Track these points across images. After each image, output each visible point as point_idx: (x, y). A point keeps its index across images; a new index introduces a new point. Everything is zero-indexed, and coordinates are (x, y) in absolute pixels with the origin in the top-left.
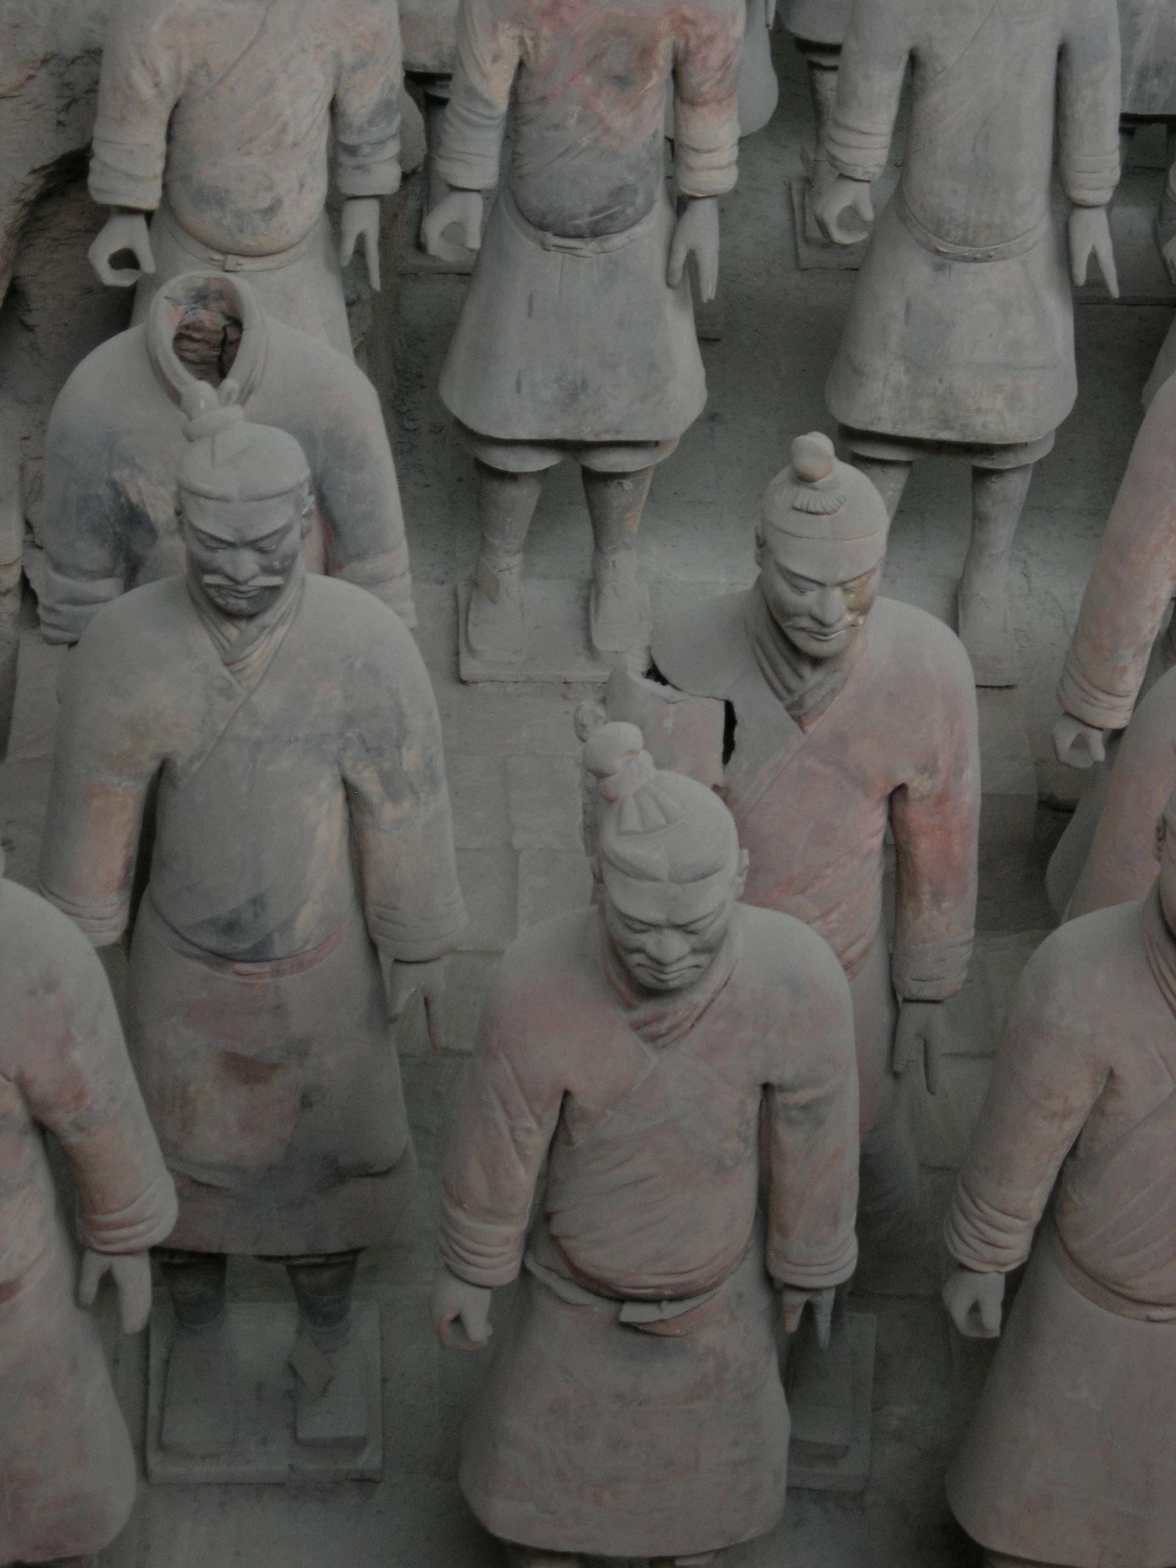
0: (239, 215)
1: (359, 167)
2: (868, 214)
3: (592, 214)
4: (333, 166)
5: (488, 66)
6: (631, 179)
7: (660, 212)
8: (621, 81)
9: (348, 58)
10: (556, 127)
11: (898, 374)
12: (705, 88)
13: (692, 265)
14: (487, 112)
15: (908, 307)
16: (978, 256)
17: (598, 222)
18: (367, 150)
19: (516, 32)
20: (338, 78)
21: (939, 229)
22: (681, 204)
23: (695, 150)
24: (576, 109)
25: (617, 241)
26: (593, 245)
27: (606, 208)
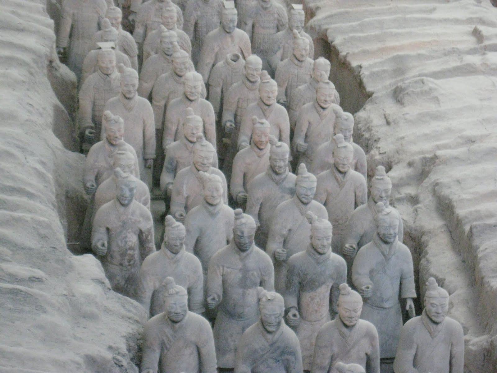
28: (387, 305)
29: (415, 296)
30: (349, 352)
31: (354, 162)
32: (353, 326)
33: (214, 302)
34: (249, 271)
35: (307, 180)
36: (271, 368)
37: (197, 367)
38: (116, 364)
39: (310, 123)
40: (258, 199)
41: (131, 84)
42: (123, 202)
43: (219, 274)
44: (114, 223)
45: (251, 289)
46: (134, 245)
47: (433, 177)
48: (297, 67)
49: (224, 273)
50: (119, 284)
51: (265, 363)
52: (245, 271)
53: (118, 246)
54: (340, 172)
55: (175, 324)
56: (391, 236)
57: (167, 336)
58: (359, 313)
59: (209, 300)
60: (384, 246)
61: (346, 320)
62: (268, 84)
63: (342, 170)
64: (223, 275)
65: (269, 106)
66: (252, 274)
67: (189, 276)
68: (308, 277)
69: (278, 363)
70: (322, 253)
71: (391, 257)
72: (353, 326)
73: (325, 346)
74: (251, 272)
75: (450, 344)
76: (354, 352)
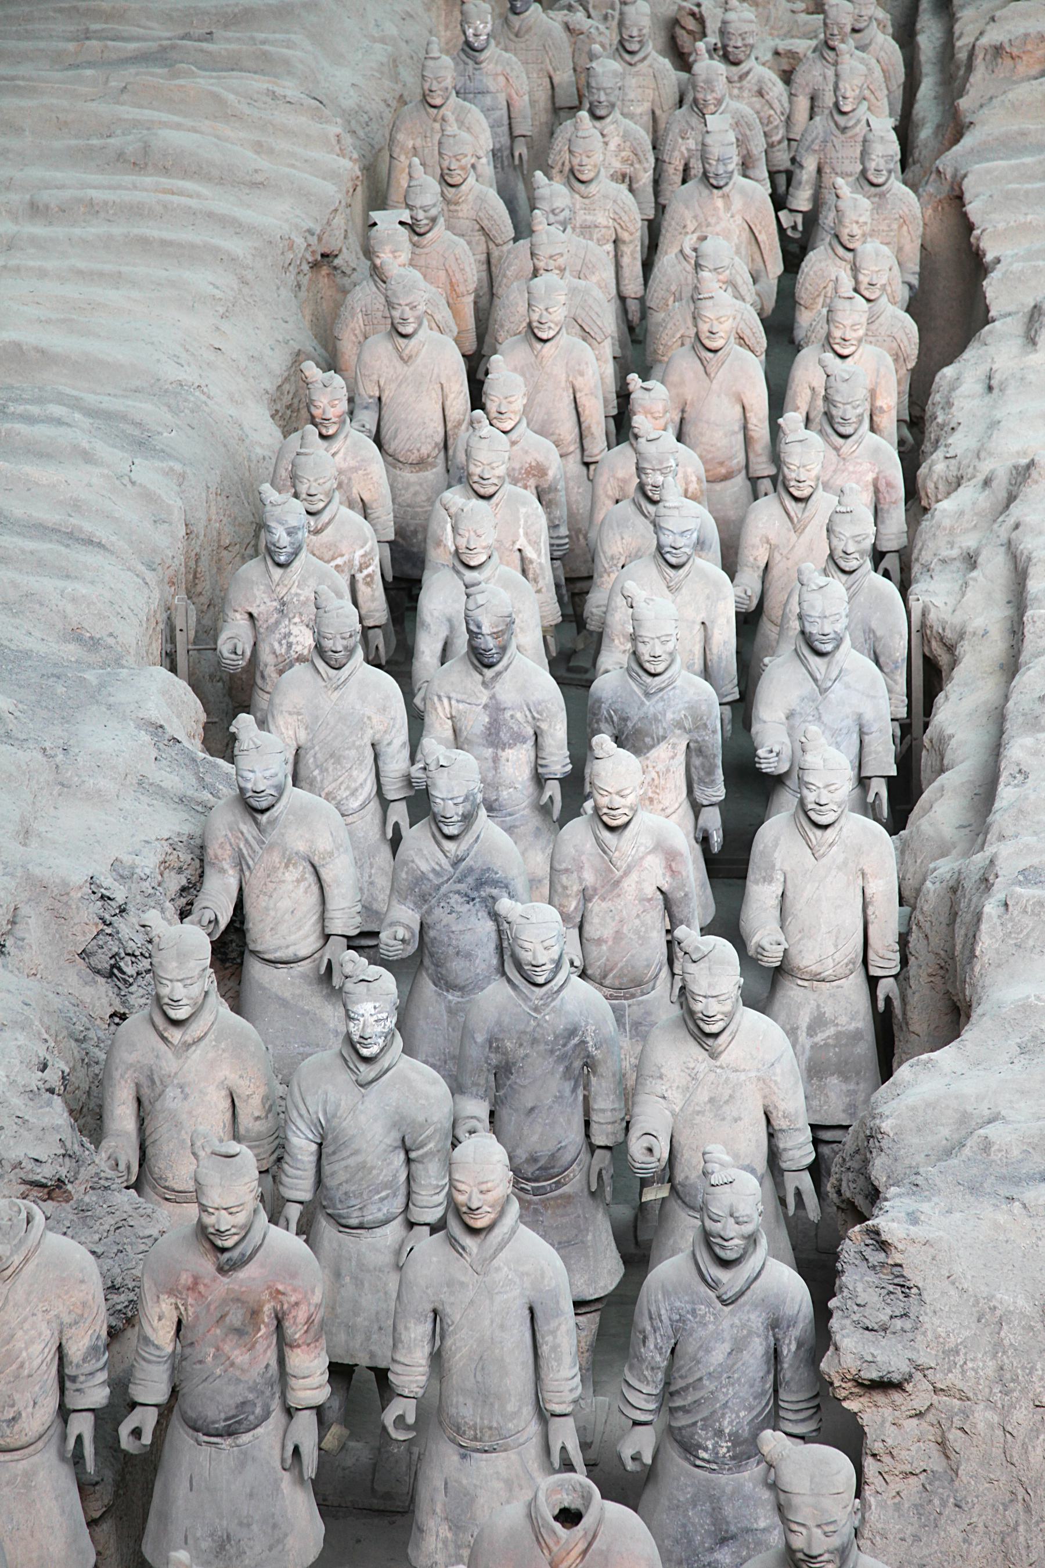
1: (78, 1390)
2: (411, 1419)
3: (226, 1420)
5: (155, 1323)
6: (251, 1396)
7: (277, 1415)
8: (239, 1332)
10: (200, 1362)
11: (444, 1531)
12: (297, 1336)
14: (157, 1353)
15: (446, 1484)
17: (229, 1426)
18: (82, 1378)
19: (173, 1301)
21: (458, 1430)
22: (290, 1412)
24: (212, 1351)
25: (245, 1438)
26: (229, 1441)
27: (234, 1417)
29: (894, 773)
30: (617, 883)
31: (870, 477)
35: (676, 512)
36: (458, 913)
37: (318, 909)
40: (612, 558)
43: (441, 715)
44: (263, 605)
45: (510, 747)
52: (495, 709)
54: (797, 499)
55: (258, 816)
57: (247, 841)
60: (814, 661)
62: (709, 303)
63: (796, 493)
64: (452, 718)
65: (715, 351)
66: (512, 717)
67: (369, 718)
68: (630, 724)
73: (567, 870)
74: (508, 714)
76: (629, 885)
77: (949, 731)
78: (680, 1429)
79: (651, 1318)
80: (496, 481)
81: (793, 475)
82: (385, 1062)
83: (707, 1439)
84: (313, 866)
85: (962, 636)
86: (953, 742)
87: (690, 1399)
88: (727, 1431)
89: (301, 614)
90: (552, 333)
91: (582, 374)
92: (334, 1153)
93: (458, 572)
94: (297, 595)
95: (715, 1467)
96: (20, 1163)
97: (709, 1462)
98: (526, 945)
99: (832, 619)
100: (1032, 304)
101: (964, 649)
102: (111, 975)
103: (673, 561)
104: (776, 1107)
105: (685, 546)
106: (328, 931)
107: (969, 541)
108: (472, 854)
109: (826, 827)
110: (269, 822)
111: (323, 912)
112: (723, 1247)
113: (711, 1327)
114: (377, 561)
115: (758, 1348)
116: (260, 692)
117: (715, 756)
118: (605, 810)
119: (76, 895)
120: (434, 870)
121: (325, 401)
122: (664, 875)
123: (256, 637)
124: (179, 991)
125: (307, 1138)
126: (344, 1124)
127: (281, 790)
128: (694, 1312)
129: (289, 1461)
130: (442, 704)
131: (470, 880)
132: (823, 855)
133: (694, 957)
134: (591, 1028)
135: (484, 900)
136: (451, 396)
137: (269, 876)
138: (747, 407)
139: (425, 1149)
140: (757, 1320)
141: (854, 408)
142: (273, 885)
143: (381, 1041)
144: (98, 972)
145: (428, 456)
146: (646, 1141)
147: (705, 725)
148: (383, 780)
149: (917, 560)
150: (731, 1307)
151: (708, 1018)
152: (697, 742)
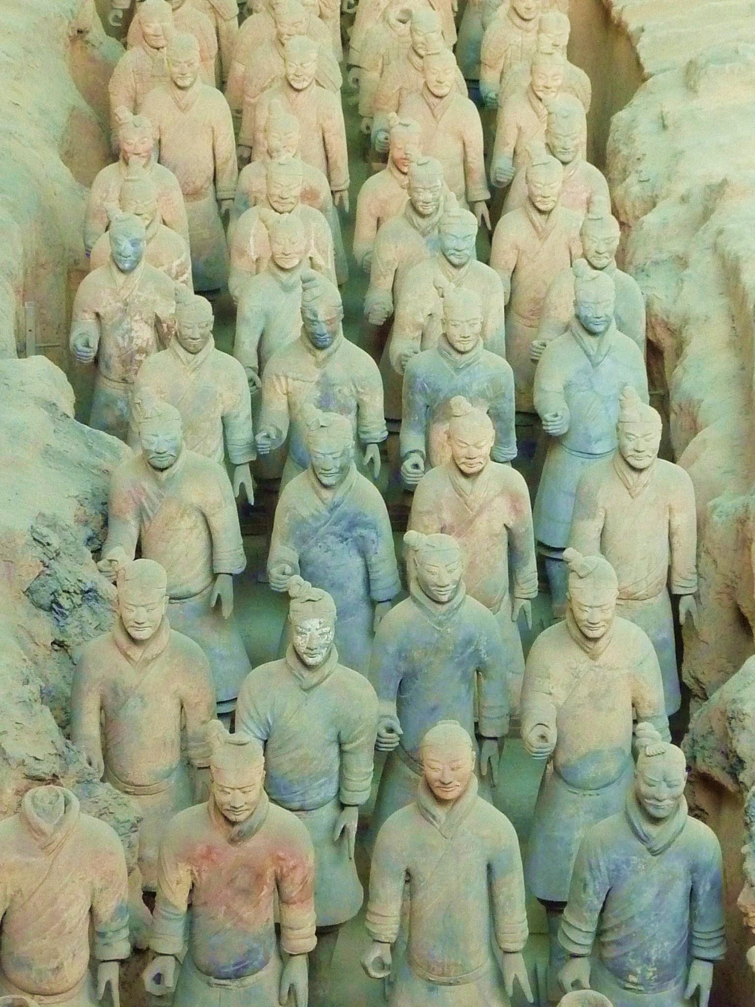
0: (40, 972)
3: (236, 965)
4: (93, 945)
6: (255, 945)
7: (274, 962)
9: (98, 885)
12: (293, 895)
13: (292, 991)
16: (451, 982)
17: (238, 970)
18: (110, 934)
19: (189, 868)
20: (93, 896)
23: (291, 928)
25: (250, 980)
26: (237, 982)
27: (243, 962)
28: (598, 449)
30: (471, 522)
32: (479, 472)
33: (267, 442)
34: (334, 385)
37: (207, 552)
38: (35, 539)
39: (520, 129)
41: (185, 62)
42: (121, 266)
43: (279, 390)
44: (108, 306)
46: (147, 344)
47: (716, 221)
48: (520, 31)
49: (289, 390)
50: (122, 416)
51: (319, 544)
52: (326, 385)
53: (118, 346)
54: (540, 212)
55: (159, 473)
56: (598, 320)
58: (486, 450)
59: (259, 438)
60: (589, 340)
61: (463, 463)
63: (542, 207)
64: (287, 393)
65: (441, 97)
66: (340, 391)
67: (221, 395)
68: (441, 396)
69: (345, 543)
70: (462, 350)
71: (601, 358)
72: (479, 472)
73: (429, 512)
74: (336, 389)
75: (667, 508)
77: (697, 397)
78: (613, 959)
79: (591, 869)
80: (293, 200)
81: (540, 192)
82: (326, 670)
83: (638, 966)
84: (204, 515)
85: (686, 321)
86: (704, 405)
87: (623, 933)
88: (654, 958)
89: (141, 314)
90: (305, 84)
91: (330, 118)
92: (280, 748)
93: (274, 275)
94: (137, 296)
95: (642, 988)
96: (24, 761)
97: (636, 984)
98: (434, 569)
99: (604, 304)
100: (688, 60)
101: (690, 331)
102: (51, 609)
103: (456, 261)
104: (642, 698)
105: (467, 249)
106: (217, 570)
107: (676, 247)
108: (345, 501)
109: (640, 471)
110: (168, 479)
111: (212, 555)
112: (657, 807)
113: (642, 874)
114: (190, 270)
115: (680, 889)
116: (105, 381)
117: (511, 420)
118: (463, 460)
119: (21, 542)
120: (313, 515)
121: (136, 139)
122: (509, 513)
123: (101, 333)
124: (142, 615)
125: (256, 737)
126: (289, 724)
127: (178, 450)
128: (627, 862)
129: (285, 998)
130: (280, 383)
131: (344, 523)
132: (638, 495)
133: (581, 574)
134: (484, 638)
135: (355, 540)
136: (220, 139)
137: (166, 525)
138: (467, 143)
139: (358, 742)
140: (680, 867)
141: (573, 139)
142: (170, 533)
143: (324, 651)
144: (41, 607)
145: (202, 187)
146: (539, 730)
147: (503, 395)
148: (230, 448)
149: (631, 263)
150: (659, 856)
151: (592, 625)
152: (496, 408)
